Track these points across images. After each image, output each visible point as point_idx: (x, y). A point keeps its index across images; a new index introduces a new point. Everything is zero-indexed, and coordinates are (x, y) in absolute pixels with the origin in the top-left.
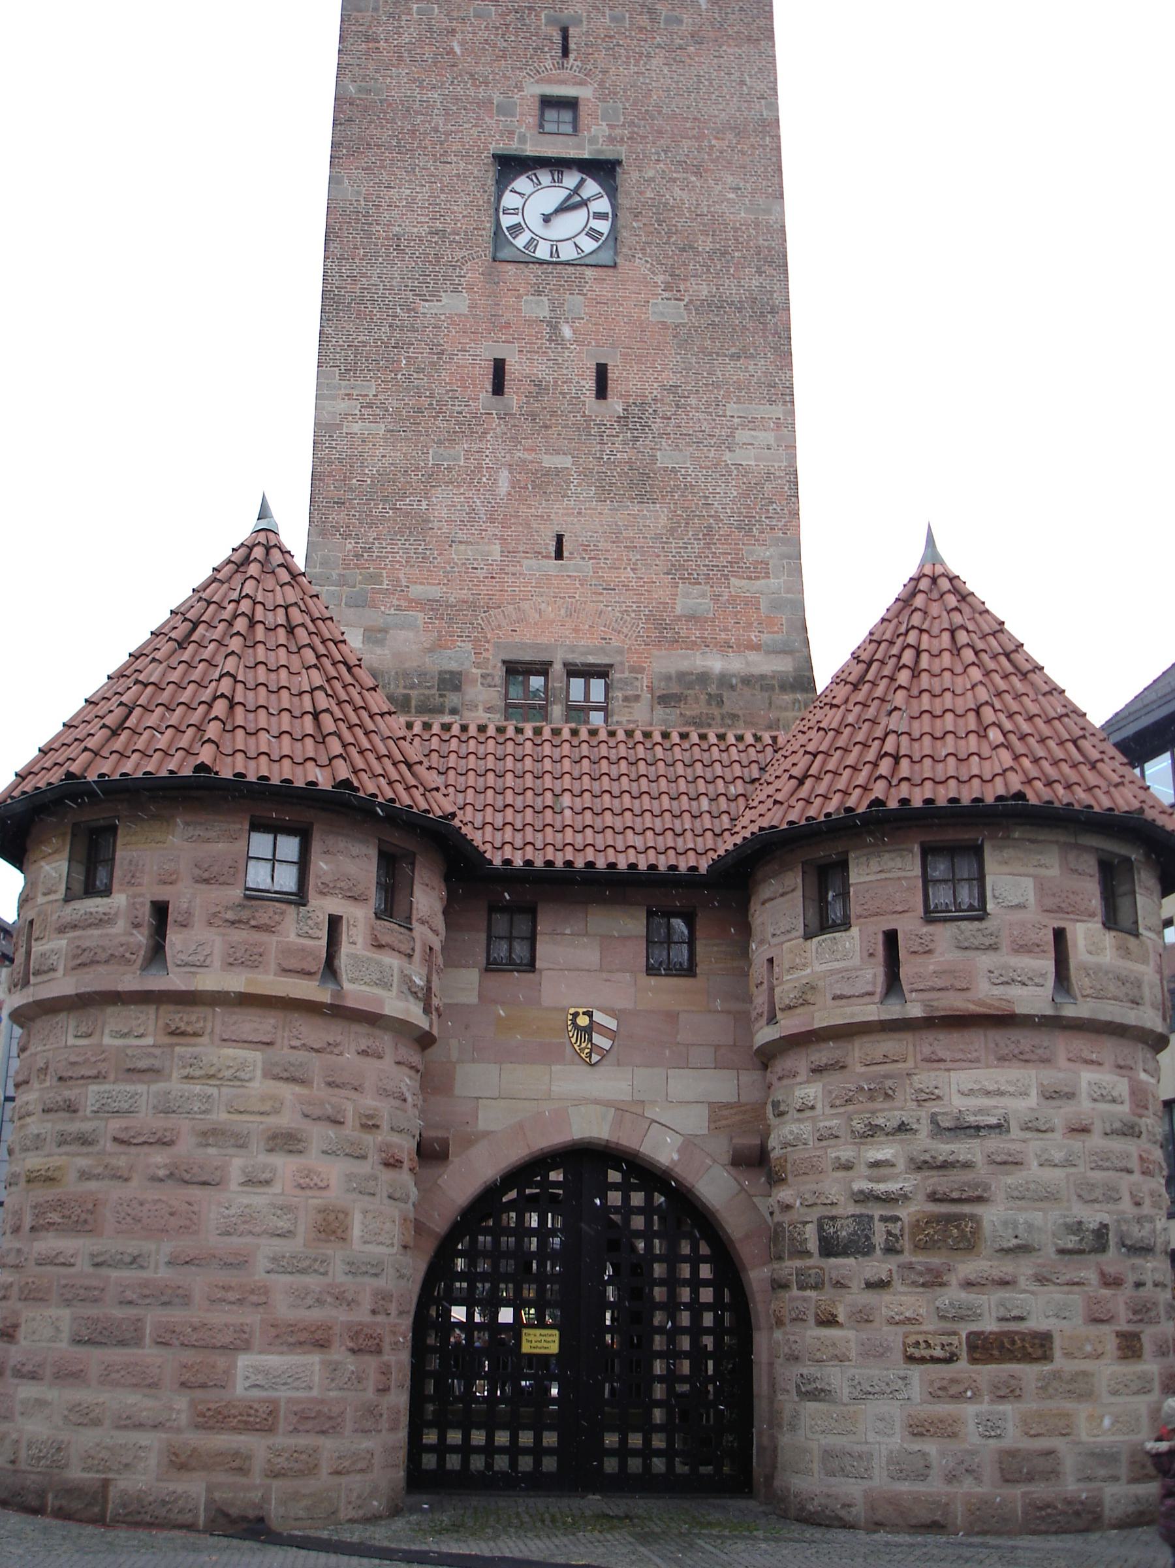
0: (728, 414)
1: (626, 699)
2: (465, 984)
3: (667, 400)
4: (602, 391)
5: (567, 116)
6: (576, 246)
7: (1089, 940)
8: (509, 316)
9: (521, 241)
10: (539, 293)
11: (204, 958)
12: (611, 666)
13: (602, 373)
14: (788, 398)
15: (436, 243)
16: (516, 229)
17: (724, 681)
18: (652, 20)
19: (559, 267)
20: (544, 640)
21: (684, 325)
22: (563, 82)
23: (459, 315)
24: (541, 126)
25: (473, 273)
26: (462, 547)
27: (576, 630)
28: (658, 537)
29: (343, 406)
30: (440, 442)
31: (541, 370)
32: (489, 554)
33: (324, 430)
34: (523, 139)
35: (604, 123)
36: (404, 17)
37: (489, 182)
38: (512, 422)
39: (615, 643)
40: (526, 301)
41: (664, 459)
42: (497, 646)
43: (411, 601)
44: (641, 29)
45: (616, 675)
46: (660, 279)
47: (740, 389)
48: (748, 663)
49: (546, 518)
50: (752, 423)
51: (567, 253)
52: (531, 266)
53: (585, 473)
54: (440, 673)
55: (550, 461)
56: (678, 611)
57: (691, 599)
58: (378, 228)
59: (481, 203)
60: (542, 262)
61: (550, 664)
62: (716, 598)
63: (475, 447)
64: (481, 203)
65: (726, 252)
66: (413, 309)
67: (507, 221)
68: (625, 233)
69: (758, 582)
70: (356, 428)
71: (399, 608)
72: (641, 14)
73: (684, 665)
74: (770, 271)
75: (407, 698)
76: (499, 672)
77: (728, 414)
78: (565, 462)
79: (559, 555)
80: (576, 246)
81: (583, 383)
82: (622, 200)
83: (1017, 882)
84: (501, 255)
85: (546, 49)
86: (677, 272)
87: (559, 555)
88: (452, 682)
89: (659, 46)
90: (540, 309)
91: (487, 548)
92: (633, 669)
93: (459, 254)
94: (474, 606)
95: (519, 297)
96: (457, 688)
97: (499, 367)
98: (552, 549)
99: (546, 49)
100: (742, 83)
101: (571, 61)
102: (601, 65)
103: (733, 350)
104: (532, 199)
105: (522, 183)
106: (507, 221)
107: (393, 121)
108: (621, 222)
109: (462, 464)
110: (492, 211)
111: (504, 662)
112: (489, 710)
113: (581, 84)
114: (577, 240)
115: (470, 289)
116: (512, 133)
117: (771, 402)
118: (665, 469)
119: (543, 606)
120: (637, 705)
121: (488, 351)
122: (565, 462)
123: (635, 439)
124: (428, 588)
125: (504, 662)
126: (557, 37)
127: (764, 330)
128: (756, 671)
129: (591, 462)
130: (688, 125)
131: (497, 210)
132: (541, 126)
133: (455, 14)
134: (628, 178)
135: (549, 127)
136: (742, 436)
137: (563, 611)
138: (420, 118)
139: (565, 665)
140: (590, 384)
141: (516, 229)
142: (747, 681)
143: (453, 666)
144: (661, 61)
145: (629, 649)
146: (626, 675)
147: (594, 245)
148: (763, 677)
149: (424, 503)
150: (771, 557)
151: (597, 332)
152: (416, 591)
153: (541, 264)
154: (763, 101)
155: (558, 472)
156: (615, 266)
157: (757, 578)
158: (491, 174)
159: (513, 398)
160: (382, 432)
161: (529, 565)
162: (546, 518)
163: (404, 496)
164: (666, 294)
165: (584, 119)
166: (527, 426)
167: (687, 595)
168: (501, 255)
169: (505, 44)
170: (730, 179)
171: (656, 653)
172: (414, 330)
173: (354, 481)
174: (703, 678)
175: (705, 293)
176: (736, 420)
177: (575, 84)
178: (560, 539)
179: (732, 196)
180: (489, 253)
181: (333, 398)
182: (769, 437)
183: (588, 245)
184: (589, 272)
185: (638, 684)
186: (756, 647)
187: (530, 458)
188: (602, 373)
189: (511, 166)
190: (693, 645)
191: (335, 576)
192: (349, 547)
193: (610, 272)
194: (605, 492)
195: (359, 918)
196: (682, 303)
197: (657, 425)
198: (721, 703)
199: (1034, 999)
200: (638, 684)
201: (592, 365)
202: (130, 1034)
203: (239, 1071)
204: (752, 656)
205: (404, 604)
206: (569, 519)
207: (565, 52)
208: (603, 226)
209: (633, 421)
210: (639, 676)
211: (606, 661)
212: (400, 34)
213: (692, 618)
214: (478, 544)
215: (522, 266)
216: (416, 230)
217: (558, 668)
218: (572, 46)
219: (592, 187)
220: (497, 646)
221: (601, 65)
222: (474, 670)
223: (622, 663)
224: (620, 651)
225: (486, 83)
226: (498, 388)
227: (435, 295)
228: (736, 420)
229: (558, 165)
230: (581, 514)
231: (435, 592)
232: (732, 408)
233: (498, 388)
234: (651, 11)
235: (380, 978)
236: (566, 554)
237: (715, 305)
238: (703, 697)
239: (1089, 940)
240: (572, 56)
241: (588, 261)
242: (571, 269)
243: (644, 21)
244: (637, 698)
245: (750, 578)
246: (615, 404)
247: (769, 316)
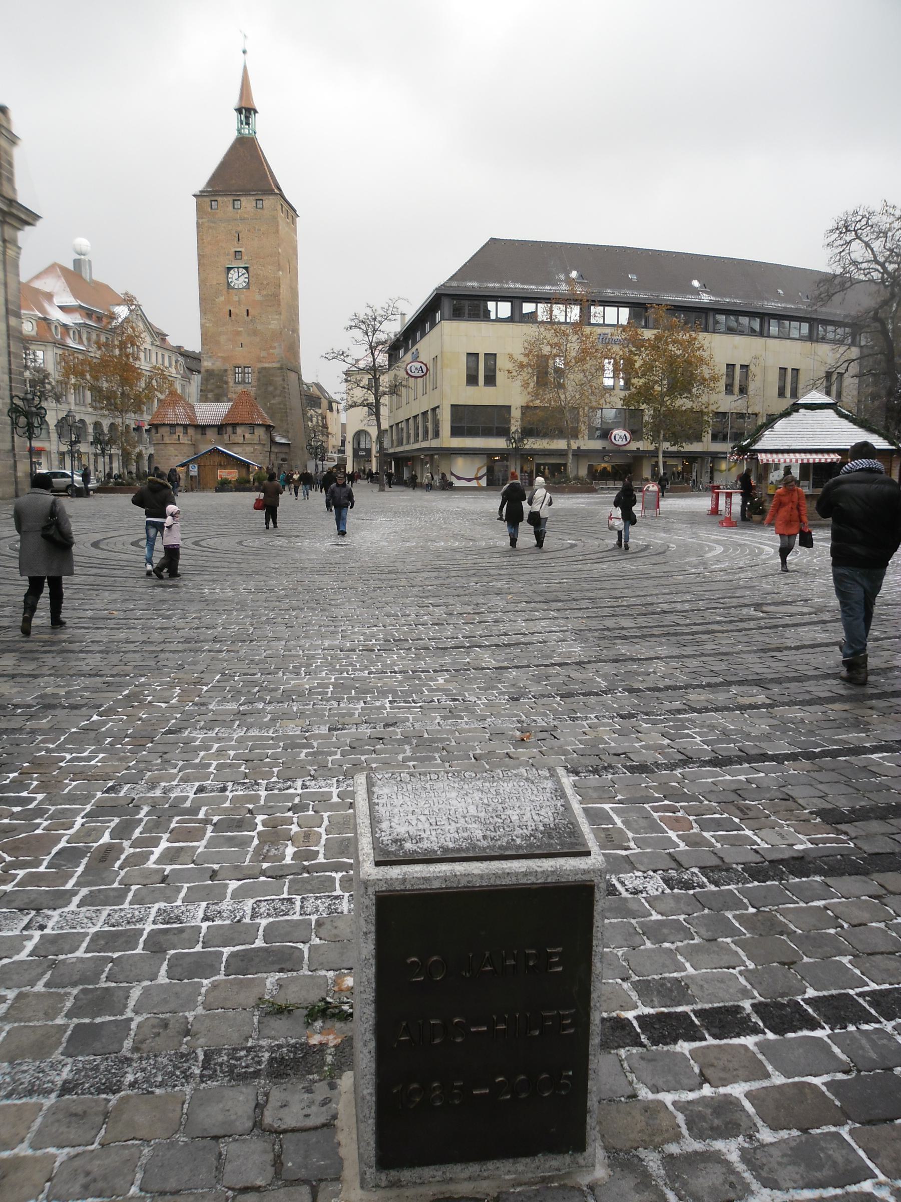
2: (199, 436)
7: (247, 436)
11: (167, 440)
17: (269, 368)
25: (224, 292)
31: (237, 311)
33: (202, 326)
41: (259, 327)
51: (241, 287)
55: (240, 329)
57: (263, 354)
83: (239, 430)
88: (226, 371)
90: (236, 298)
105: (232, 272)
134: (250, 269)
174: (265, 368)
189: (229, 269)
195: (181, 435)
199: (241, 440)
202: (161, 447)
203: (171, 450)
208: (247, 280)
219: (244, 271)
229: (238, 268)
235: (184, 440)
237: (267, 295)
239: (247, 436)
246: (250, 317)
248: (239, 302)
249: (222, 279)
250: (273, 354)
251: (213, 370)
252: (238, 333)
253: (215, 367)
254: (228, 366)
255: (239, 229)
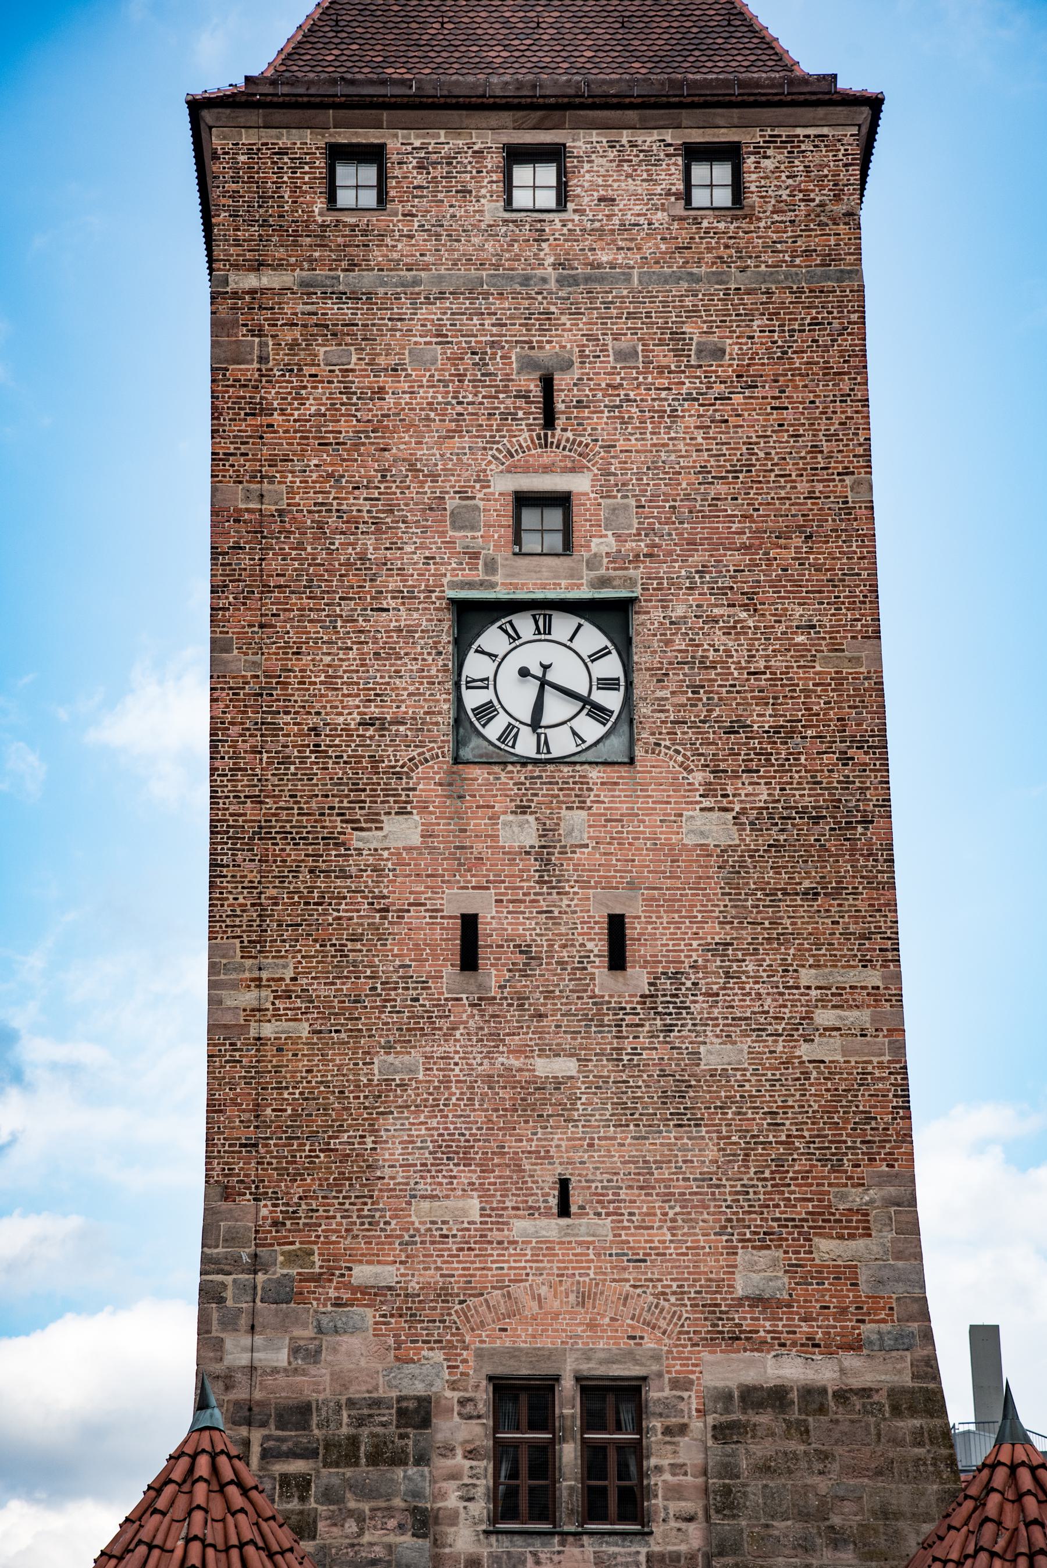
0: (803, 983)
1: (668, 1431)
3: (712, 967)
4: (617, 960)
5: (554, 517)
6: (575, 733)
8: (479, 847)
9: (493, 731)
10: (523, 810)
12: (644, 1379)
13: (616, 925)
14: (890, 955)
15: (371, 738)
16: (487, 712)
17: (813, 1397)
18: (678, 353)
19: (550, 767)
20: (546, 1343)
21: (734, 848)
22: (547, 469)
23: (409, 849)
24: (517, 540)
25: (427, 782)
26: (425, 1205)
27: (592, 1326)
28: (705, 1178)
29: (248, 998)
30: (388, 1048)
31: (527, 927)
32: (464, 1211)
33: (225, 1038)
34: (491, 567)
35: (610, 533)
36: (307, 370)
37: (445, 638)
38: (490, 1010)
39: (649, 1344)
40: (504, 824)
42: (480, 1354)
43: (354, 1289)
44: (661, 370)
45: (654, 1394)
46: (698, 777)
47: (818, 946)
48: (842, 1371)
49: (543, 1156)
50: (839, 997)
51: (561, 744)
52: (510, 768)
53: (598, 1085)
54: (400, 1399)
55: (545, 1067)
56: (740, 1292)
58: (288, 718)
59: (433, 672)
60: (525, 762)
61: (557, 1379)
62: (791, 1269)
63: (439, 1051)
64: (433, 672)
65: (791, 733)
66: (343, 844)
67: (473, 699)
68: (643, 710)
69: (852, 1244)
70: (268, 1030)
71: (338, 1303)
72: (661, 342)
73: (750, 1377)
74: (860, 756)
75: (354, 1441)
76: (484, 1396)
77: (803, 983)
78: (566, 1066)
79: (564, 1210)
80: (575, 733)
81: (590, 945)
82: (638, 657)
84: (466, 753)
85: (520, 414)
86: (723, 766)
87: (564, 1210)
88: (418, 1414)
89: (689, 398)
90: (524, 834)
91: (460, 1204)
92: (675, 1384)
93: (404, 756)
94: (444, 1294)
95: (494, 817)
96: (425, 1422)
97: (469, 924)
98: (553, 1202)
99: (520, 414)
100: (816, 450)
101: (558, 432)
102: (603, 436)
103: (806, 884)
104: (505, 670)
105: (492, 638)
106: (473, 699)
107: (300, 547)
108: (637, 692)
109: (421, 1077)
110: (449, 685)
111: (490, 1378)
112: (471, 1454)
113: (573, 470)
114: (573, 723)
115: (423, 809)
116: (475, 556)
117: (866, 963)
118: (713, 1073)
119: (544, 1290)
120: (684, 1441)
121: (456, 901)
122: (566, 1066)
123: (668, 1029)
124: (378, 1269)
125: (490, 1378)
126: (535, 389)
127: (853, 850)
128: (856, 1383)
129: (607, 1068)
130: (735, 527)
131: (457, 685)
132: (517, 540)
133: (382, 361)
134: (647, 623)
135: (531, 543)
136: (825, 1017)
137: (572, 1298)
138: (339, 539)
139: (578, 1379)
140: (598, 946)
141: (487, 712)
142: (842, 1396)
143: (419, 1389)
144: (692, 422)
145: (670, 1352)
146: (667, 1393)
147: (600, 730)
148: (865, 1392)
149: (369, 1140)
150: (872, 1201)
151: (608, 866)
152: (363, 1273)
153: (524, 764)
154: (848, 480)
155: (558, 1083)
156: (632, 761)
157: (852, 1237)
158: (446, 625)
159: (492, 975)
160: (305, 1034)
161: (521, 1226)
162: (543, 1156)
163: (341, 1130)
164: (707, 803)
165: (581, 525)
166: (513, 1014)
167: (752, 1267)
168: (466, 753)
169: (459, 409)
170: (799, 611)
171: (706, 1356)
172: (344, 875)
173: (269, 1111)
174: (776, 1397)
175: (764, 797)
176: (814, 993)
177: (565, 470)
178: (564, 1185)
179: (800, 639)
180: (449, 748)
181: (234, 986)
182: (862, 1017)
183: (591, 730)
184: (594, 774)
185: (682, 1406)
186: (855, 1345)
187: (515, 1063)
188: (616, 925)
189: (471, 616)
190: (761, 1346)
191: (245, 1258)
192: (264, 1212)
193: (623, 771)
194: (626, 1113)
196: (729, 816)
197: (699, 1006)
198: (805, 1433)
200: (682, 1406)
201: (600, 915)
204: (851, 1361)
205: (346, 1295)
206: (576, 1157)
207: (549, 420)
209: (664, 1003)
210: (685, 1395)
211: (636, 1371)
212: (302, 400)
213: (757, 1301)
214: (447, 1197)
215: (497, 769)
216: (341, 720)
217: (568, 1385)
218: (560, 406)
219: (592, 639)
220: (480, 1354)
221: (603, 436)
222: (448, 1394)
223: (660, 1375)
224: (656, 1357)
225: (434, 477)
226: (469, 959)
227: (374, 821)
228: (814, 993)
229: (544, 609)
230: (595, 1149)
231: (387, 1274)
232: (807, 976)
233: (469, 959)
234: (677, 336)
236: (574, 1209)
238: (780, 1428)
240: (560, 423)
241: (589, 756)
242: (566, 769)
243: (664, 356)
244: (683, 1429)
245: (841, 1237)
247: (860, 830)
248: (546, 855)
249: (414, 688)
250: (846, 1274)
251: (298, 1414)
252: (535, 1101)
253: (317, 1384)
254: (429, 1374)
255: (565, 339)
